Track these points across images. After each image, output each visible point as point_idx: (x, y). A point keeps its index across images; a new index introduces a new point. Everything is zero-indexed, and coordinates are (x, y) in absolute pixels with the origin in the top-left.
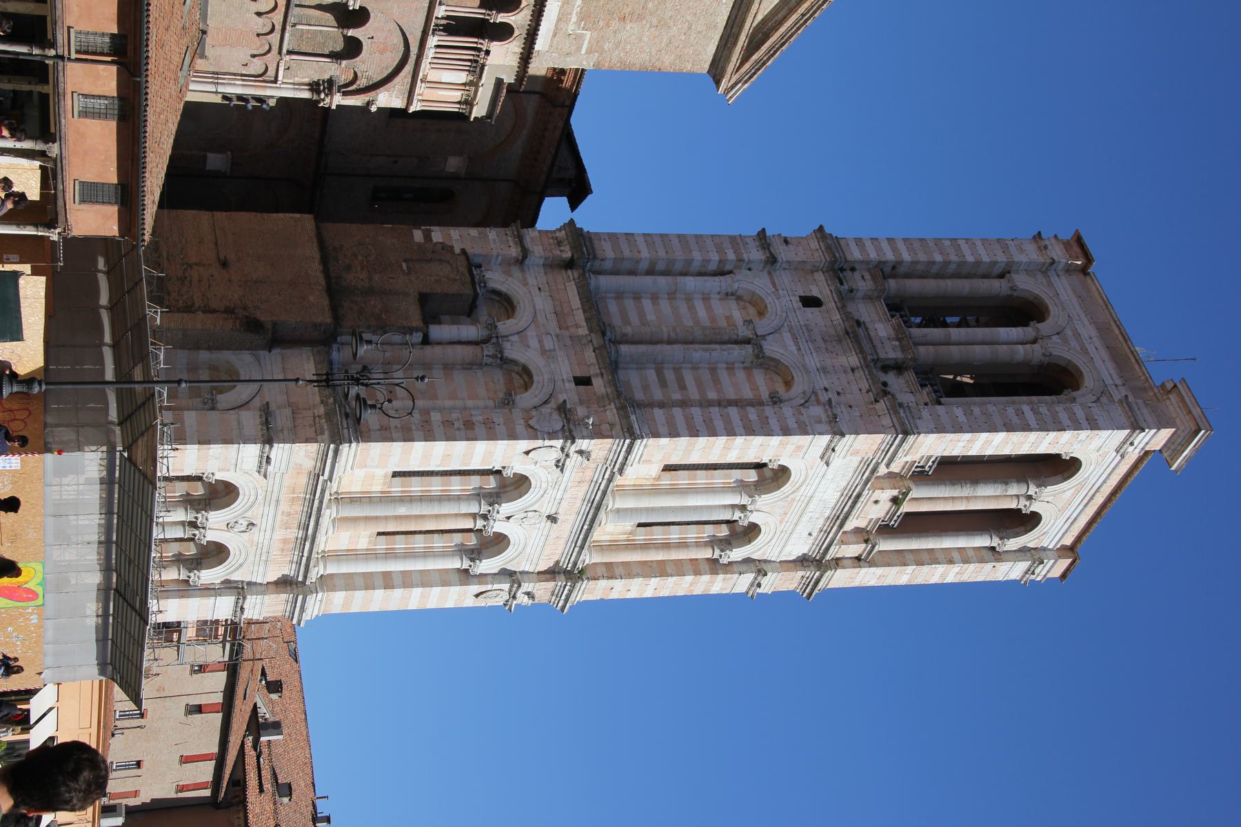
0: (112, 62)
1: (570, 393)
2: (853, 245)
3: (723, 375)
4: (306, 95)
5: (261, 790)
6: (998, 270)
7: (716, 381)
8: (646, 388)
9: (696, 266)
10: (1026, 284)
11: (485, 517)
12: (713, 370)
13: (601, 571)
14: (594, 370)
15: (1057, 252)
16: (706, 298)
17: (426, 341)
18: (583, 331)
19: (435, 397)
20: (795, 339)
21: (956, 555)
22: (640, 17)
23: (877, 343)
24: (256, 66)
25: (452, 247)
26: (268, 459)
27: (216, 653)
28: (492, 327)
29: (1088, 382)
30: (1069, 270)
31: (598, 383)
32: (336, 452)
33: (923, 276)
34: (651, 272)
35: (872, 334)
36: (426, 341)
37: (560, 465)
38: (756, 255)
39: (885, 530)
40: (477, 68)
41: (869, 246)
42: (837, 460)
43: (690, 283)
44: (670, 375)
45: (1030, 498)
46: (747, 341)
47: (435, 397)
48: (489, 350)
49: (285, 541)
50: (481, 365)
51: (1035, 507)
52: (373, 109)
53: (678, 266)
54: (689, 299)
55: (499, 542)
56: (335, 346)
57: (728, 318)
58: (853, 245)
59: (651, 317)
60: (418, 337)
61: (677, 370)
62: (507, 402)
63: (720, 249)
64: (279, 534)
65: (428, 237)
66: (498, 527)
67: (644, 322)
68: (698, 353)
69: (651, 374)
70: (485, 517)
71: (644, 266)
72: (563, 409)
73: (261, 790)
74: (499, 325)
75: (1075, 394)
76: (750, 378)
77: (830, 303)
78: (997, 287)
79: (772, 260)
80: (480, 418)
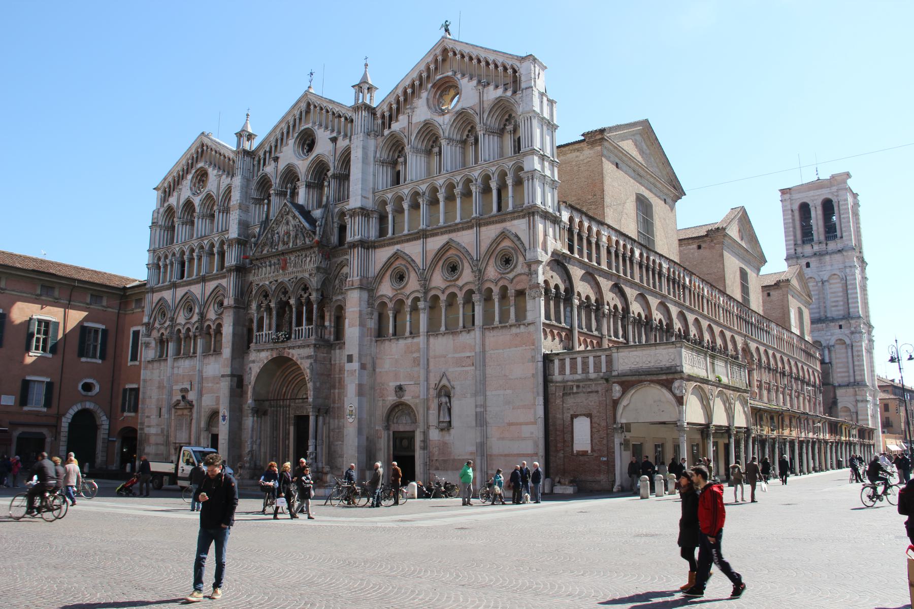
1: (845, 331)
8: (839, 311)
14: (837, 324)
18: (824, 325)
20: (821, 271)
31: (841, 323)
36: (830, 363)
44: (834, 304)
46: (823, 283)
69: (833, 309)
72: (852, 333)
77: (809, 260)
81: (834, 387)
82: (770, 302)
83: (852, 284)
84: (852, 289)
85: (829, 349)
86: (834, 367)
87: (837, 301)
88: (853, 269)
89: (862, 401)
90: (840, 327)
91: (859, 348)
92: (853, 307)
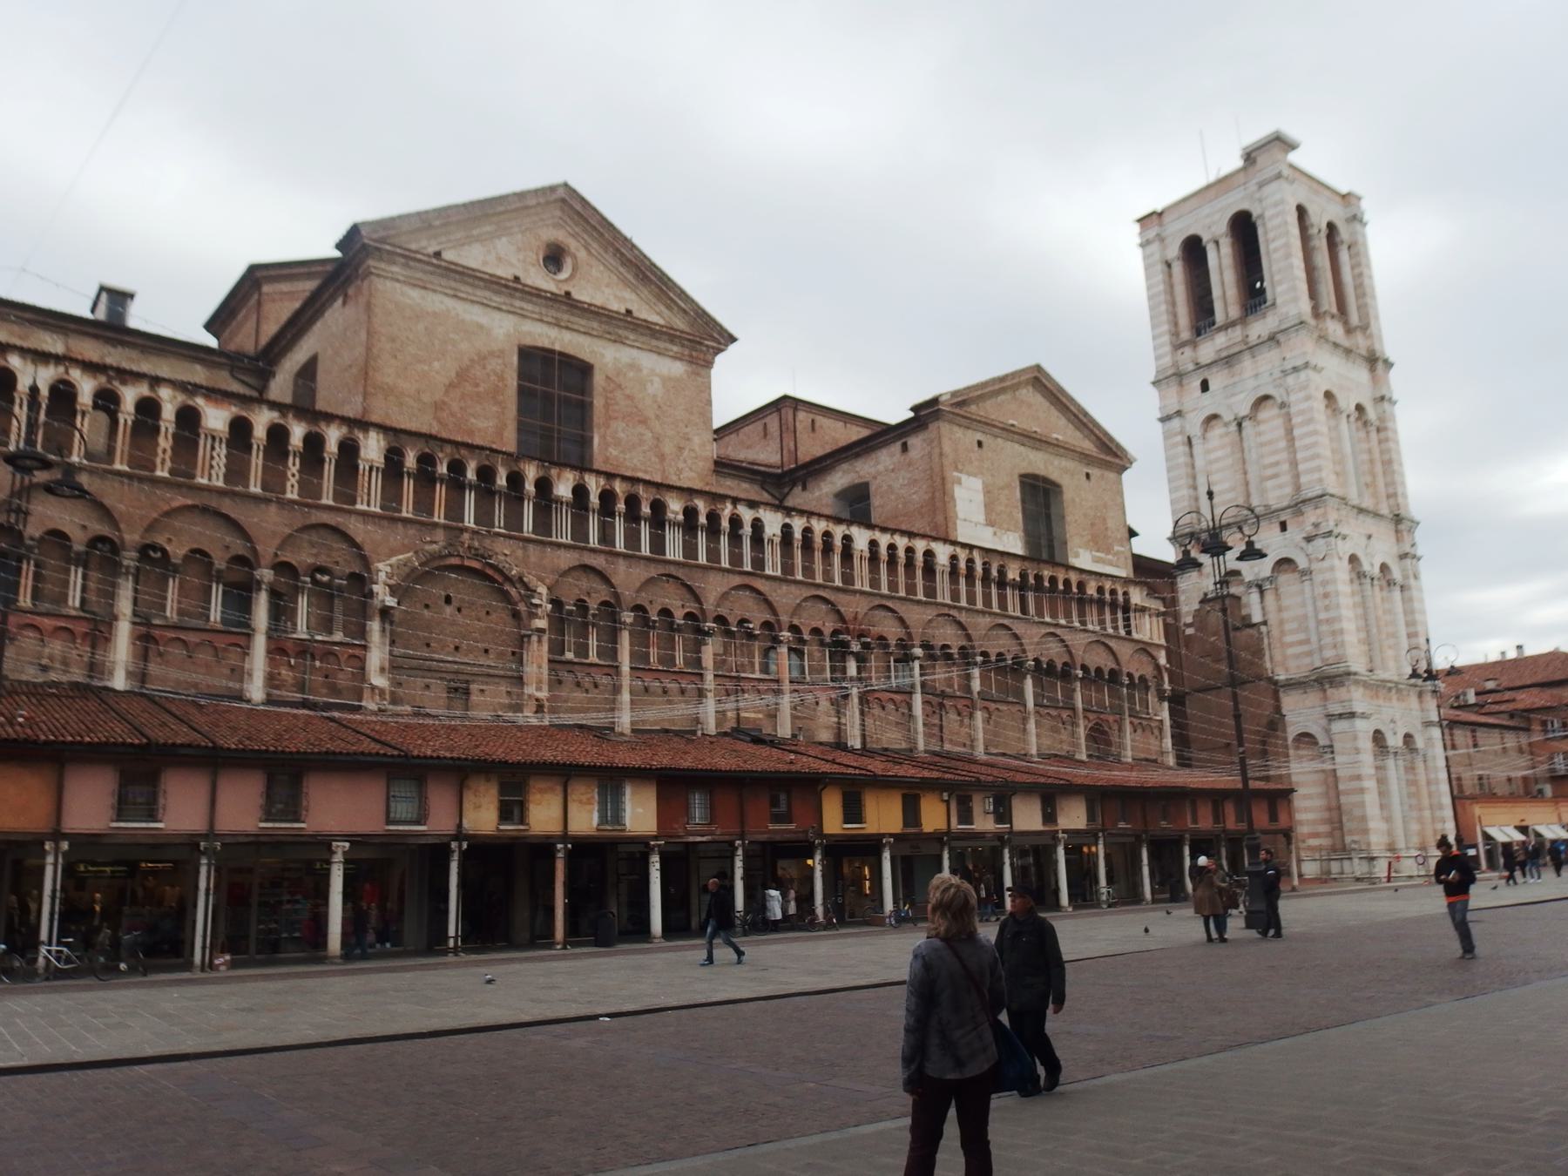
0: (1223, 806)
2: (1161, 362)
3: (1264, 438)
4: (1166, 705)
5: (1514, 700)
6: (1166, 269)
7: (1270, 443)
8: (1280, 487)
9: (1188, 459)
10: (1174, 250)
11: (1372, 579)
12: (1262, 445)
13: (1392, 501)
15: (1151, 234)
16: (1208, 452)
17: (1265, 623)
19: (1305, 617)
20: (1233, 395)
21: (1357, 271)
22: (1105, 519)
23: (1231, 343)
24: (1156, 732)
25: (1196, 611)
26: (1363, 713)
27: (1461, 736)
28: (1249, 585)
29: (1244, 206)
30: (1161, 225)
31: (1282, 519)
32: (1355, 674)
33: (1175, 315)
34: (1195, 488)
35: (1224, 346)
36: (1265, 623)
37: (1344, 538)
38: (1176, 423)
39: (1346, 323)
40: (1143, 610)
41: (1161, 351)
42: (1320, 365)
43: (1199, 463)
44: (1269, 472)
45: (1320, 231)
46: (1240, 425)
47: (1305, 617)
48: (1267, 586)
49: (1398, 699)
50: (1276, 589)
51: (1324, 226)
52: (1168, 666)
53: (1189, 470)
54: (1211, 462)
55: (1384, 568)
56: (1276, 678)
57: (1221, 436)
58: (1161, 362)
59: (1226, 485)
60: (1263, 629)
61: (1265, 467)
62: (1306, 573)
63: (1175, 445)
64: (1395, 702)
65: (1188, 625)
66: (1376, 570)
67: (1232, 489)
68: (1252, 456)
69: (1269, 484)
70: (1372, 579)
71: (1191, 492)
73: (1514, 700)
74: (1247, 580)
75: (1255, 215)
76: (1264, 421)
78: (1178, 269)
79: (1179, 413)
80: (1321, 589)
81: (1276, 688)
82: (910, 464)
83: (1301, 412)
84: (1304, 423)
85: (1259, 587)
86: (1275, 632)
87: (1277, 464)
88: (1303, 375)
89: (1341, 716)
90: (1283, 526)
91: (1328, 576)
92: (1311, 471)
